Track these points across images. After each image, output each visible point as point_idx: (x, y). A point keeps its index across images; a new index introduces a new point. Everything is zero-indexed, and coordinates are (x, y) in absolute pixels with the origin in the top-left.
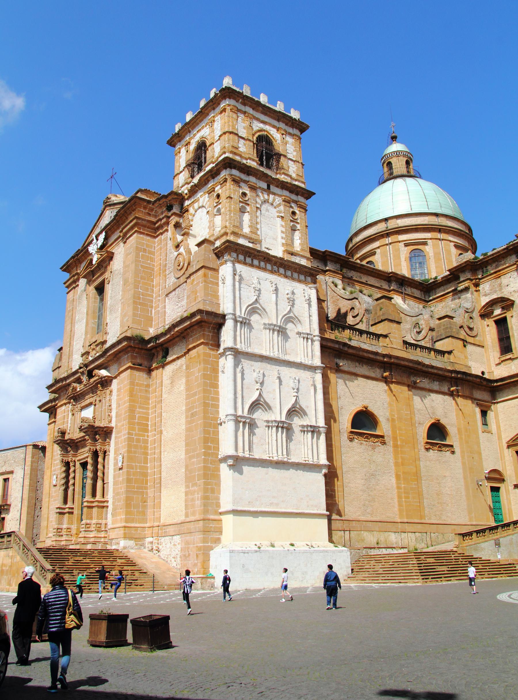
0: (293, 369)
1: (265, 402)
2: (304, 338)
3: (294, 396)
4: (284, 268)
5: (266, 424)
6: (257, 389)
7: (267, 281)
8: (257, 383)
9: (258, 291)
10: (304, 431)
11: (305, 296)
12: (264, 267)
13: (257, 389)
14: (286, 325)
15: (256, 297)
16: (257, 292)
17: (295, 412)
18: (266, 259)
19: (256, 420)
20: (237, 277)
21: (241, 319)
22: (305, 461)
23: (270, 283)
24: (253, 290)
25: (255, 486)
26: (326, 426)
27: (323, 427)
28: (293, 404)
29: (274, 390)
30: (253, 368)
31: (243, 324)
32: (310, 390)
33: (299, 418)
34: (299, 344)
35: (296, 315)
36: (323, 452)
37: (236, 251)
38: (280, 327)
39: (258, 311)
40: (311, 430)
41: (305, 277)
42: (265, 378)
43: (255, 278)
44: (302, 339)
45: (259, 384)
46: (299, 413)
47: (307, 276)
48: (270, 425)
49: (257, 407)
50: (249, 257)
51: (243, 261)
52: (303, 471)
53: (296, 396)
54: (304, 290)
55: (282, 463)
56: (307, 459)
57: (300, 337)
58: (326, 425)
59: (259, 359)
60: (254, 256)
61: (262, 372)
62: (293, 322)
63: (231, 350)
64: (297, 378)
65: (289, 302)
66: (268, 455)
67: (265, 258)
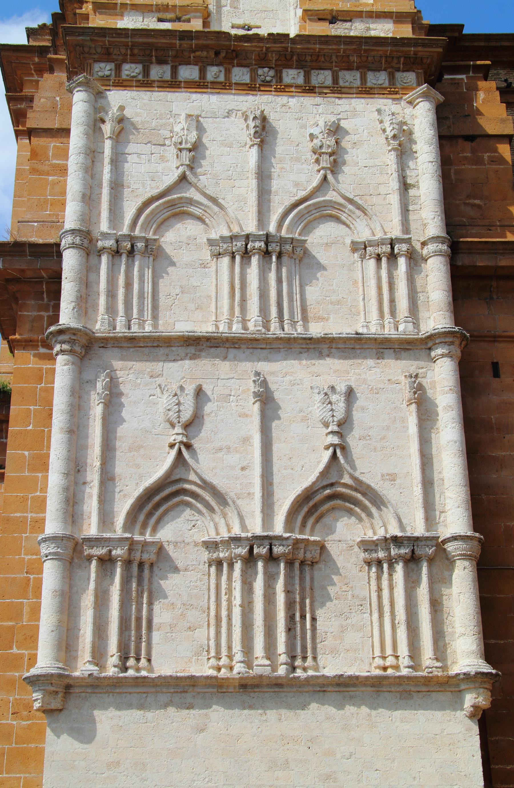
0: (329, 361)
1: (207, 485)
2: (378, 258)
3: (327, 448)
4: (301, 65)
5: (205, 555)
6: (172, 446)
7: (232, 118)
8: (173, 426)
9: (190, 150)
10: (379, 563)
11: (384, 131)
12: (222, 78)
13: (172, 446)
14: (307, 229)
15: (181, 169)
16: (186, 157)
17: (339, 502)
18: (223, 54)
19: (170, 550)
20: (107, 128)
21: (110, 243)
22: (385, 669)
23: (242, 120)
24: (172, 151)
25: (143, 780)
26: (477, 535)
27: (454, 538)
28: (324, 474)
29: (246, 440)
30: (159, 380)
31: (124, 258)
32: (404, 420)
33: (360, 519)
34: (360, 284)
35: (348, 195)
36: (463, 630)
37: (108, 54)
38: (268, 239)
39: (192, 209)
40: (400, 556)
41: (392, 78)
42: (208, 408)
43: (183, 117)
44: (372, 263)
45: (178, 429)
46: (356, 502)
47: (398, 70)
48: (221, 555)
49: (177, 504)
50: (161, 62)
51: (140, 77)
52: (373, 707)
53: (334, 446)
54: (379, 111)
55: (269, 686)
56: (390, 661)
57: (363, 258)
58: (475, 530)
59: (182, 351)
60: (176, 57)
61: (190, 389)
62: (338, 219)
63: (61, 338)
64: (342, 388)
65: (317, 161)
66: (213, 661)
67: (217, 54)
